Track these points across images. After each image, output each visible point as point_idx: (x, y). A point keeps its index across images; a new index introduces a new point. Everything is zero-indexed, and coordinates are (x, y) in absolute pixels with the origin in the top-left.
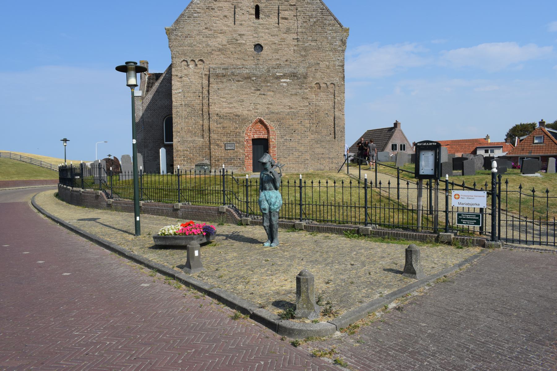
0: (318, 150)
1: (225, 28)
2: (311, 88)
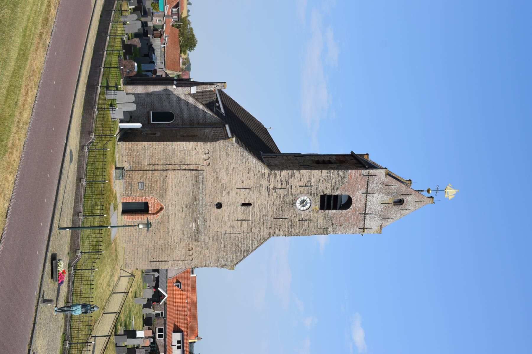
0: (140, 251)
1: (234, 182)
2: (189, 244)
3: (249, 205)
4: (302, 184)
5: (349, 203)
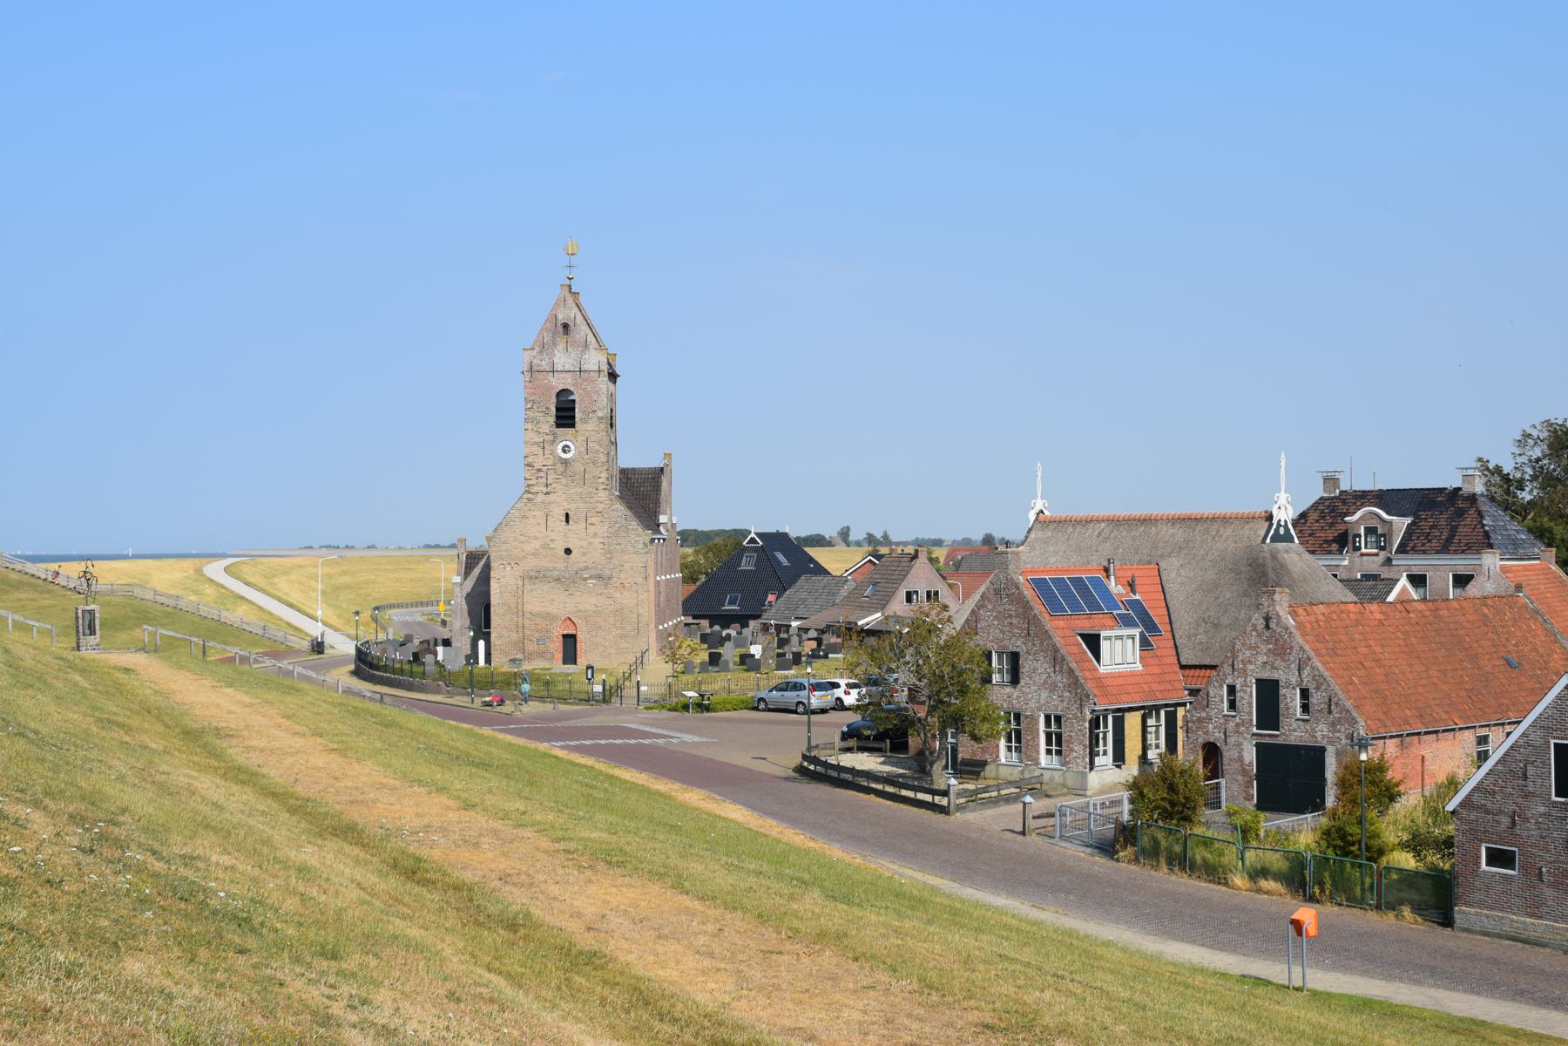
5: (563, 393)
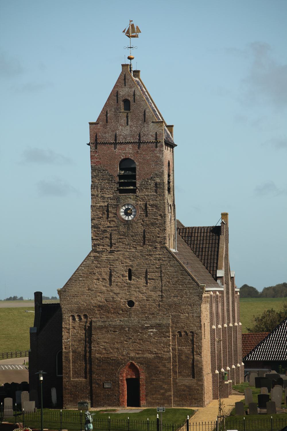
3: (130, 271)
4: (105, 216)
